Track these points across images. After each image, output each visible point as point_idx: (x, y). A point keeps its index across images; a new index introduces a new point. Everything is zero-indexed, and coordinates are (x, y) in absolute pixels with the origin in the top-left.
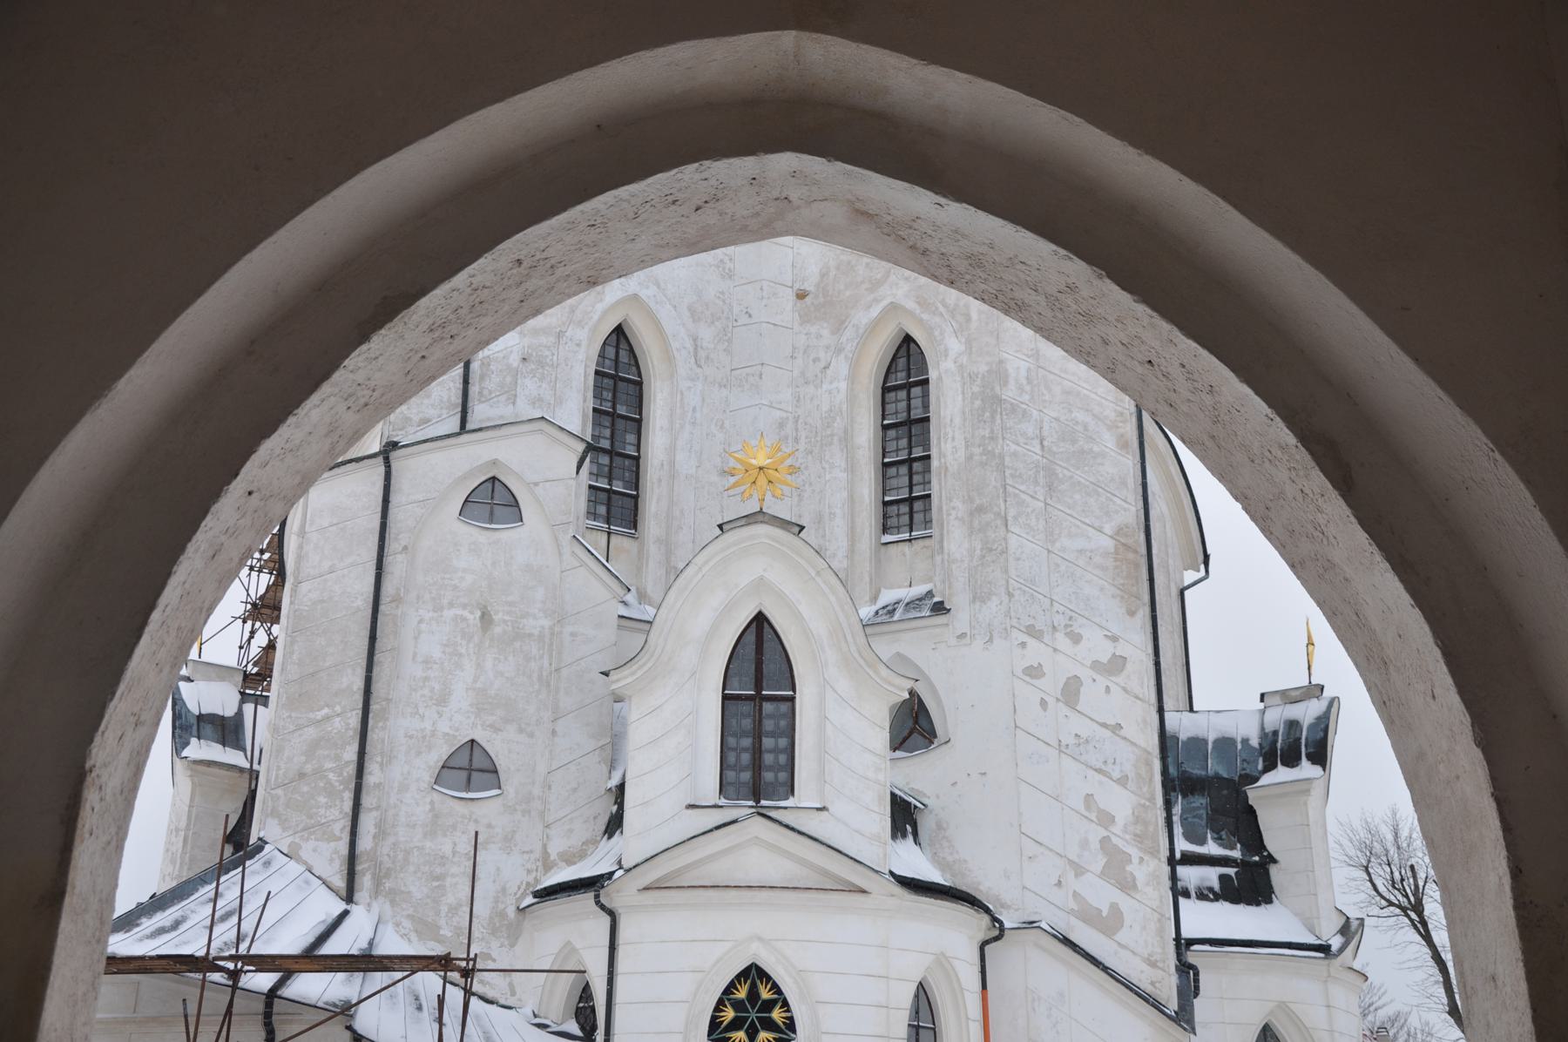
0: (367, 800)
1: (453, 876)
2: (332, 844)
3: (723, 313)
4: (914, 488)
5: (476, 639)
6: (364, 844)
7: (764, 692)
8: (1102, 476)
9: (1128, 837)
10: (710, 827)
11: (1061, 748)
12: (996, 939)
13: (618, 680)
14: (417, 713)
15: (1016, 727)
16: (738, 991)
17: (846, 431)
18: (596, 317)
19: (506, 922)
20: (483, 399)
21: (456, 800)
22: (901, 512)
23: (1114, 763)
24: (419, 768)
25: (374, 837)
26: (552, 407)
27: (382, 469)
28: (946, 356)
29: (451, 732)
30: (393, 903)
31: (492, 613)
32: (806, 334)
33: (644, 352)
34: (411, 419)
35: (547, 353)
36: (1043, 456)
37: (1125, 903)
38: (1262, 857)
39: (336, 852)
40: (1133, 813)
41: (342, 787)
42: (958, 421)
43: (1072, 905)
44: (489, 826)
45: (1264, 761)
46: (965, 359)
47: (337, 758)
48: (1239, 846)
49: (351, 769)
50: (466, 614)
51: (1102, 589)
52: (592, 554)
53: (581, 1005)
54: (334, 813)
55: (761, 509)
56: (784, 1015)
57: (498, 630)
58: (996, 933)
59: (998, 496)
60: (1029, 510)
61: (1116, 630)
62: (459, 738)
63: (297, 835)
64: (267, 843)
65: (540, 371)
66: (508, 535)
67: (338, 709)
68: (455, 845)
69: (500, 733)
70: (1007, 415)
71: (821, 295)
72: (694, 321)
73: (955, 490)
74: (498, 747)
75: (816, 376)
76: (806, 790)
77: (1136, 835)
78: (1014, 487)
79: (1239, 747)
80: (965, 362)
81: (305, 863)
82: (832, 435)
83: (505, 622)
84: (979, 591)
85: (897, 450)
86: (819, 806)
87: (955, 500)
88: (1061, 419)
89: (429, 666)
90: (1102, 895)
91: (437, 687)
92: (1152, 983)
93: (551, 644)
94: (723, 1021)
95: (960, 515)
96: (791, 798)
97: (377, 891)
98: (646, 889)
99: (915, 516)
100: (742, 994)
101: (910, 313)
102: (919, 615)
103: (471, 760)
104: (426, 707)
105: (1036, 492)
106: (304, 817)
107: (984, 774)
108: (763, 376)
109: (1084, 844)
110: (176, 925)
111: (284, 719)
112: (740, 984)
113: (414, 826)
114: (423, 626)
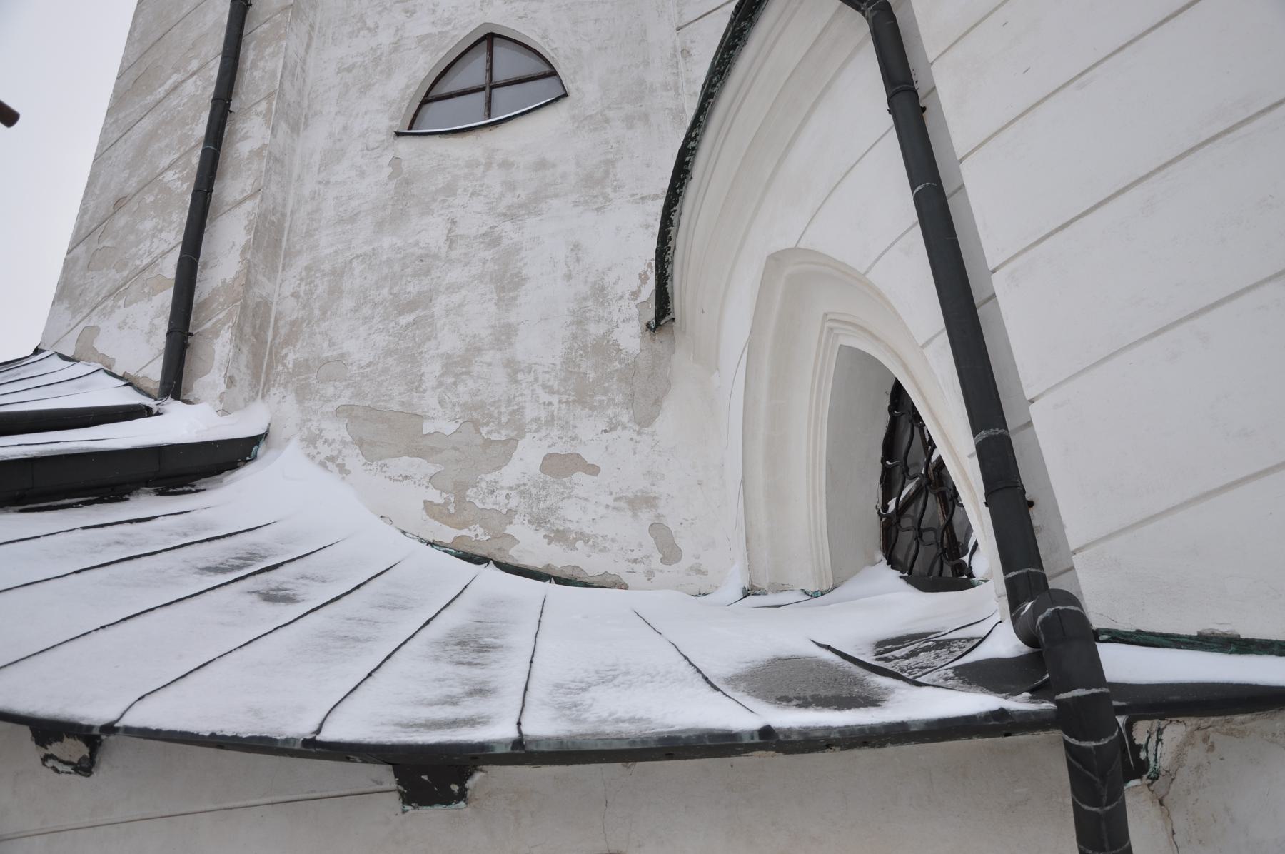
1: (453, 288)
19: (616, 365)
29: (435, 30)
30: (303, 393)
62: (455, 33)
68: (454, 222)
103: (490, 70)
113: (353, 218)
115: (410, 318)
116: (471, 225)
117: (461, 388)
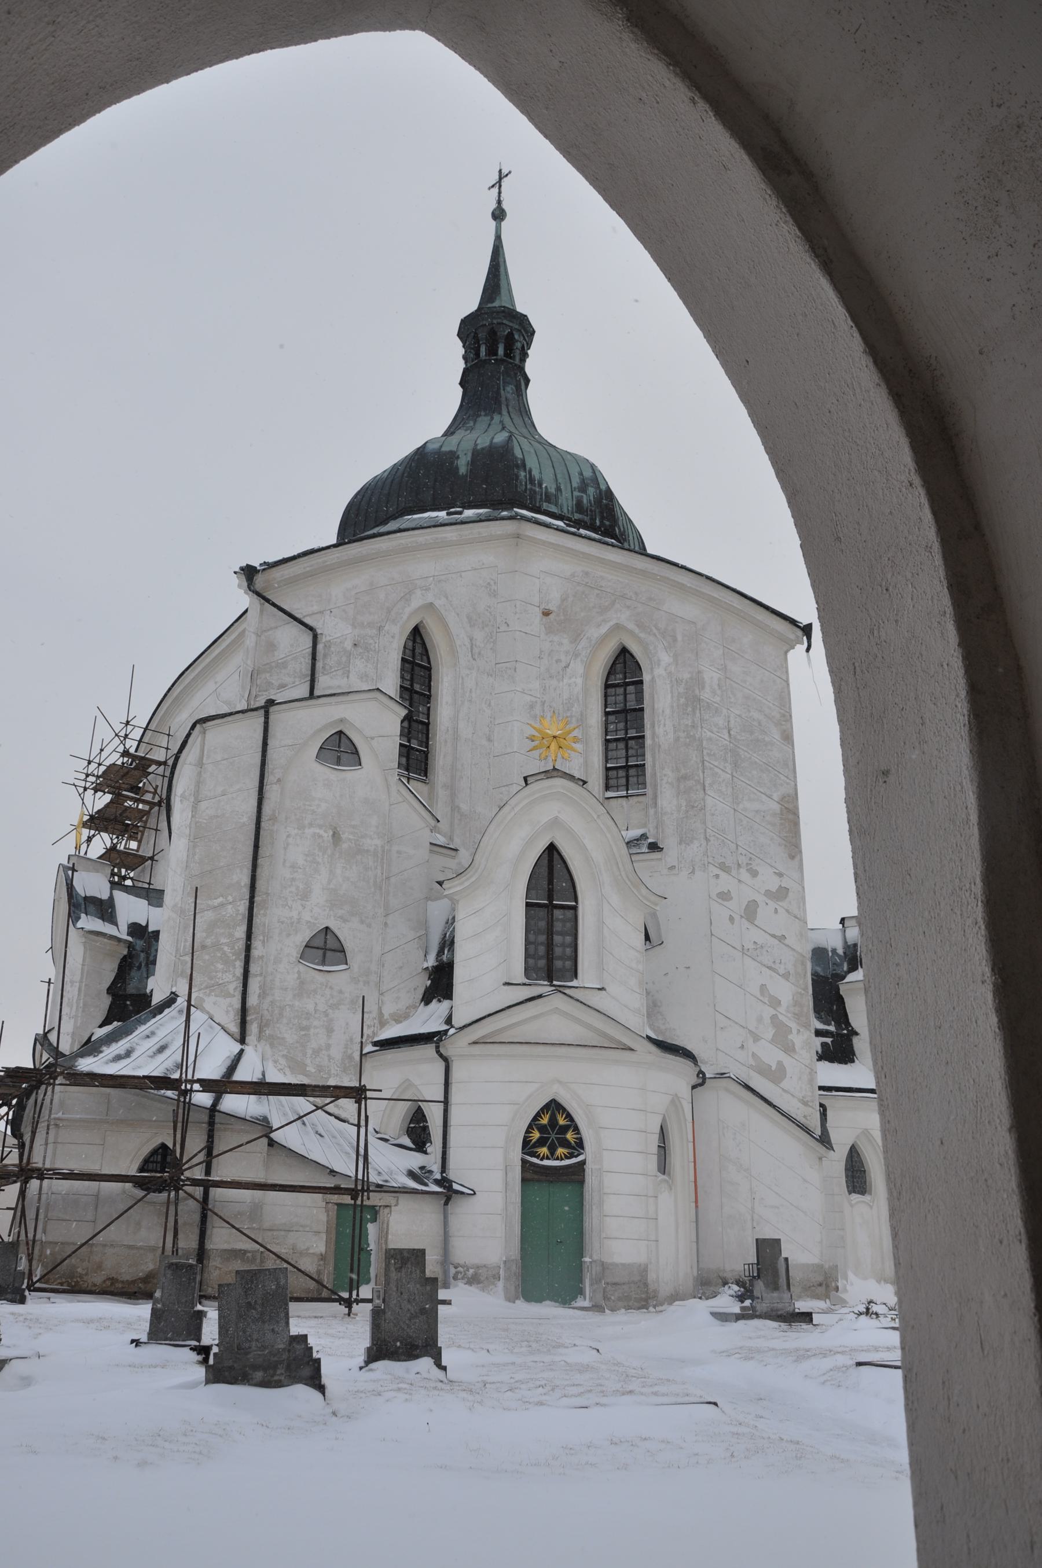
0: (254, 968)
1: (316, 1027)
2: (228, 1000)
3: (490, 621)
4: (630, 759)
5: (329, 852)
6: (252, 1000)
7: (554, 902)
8: (771, 759)
9: (789, 1015)
10: (521, 1000)
11: (744, 951)
12: (702, 1084)
13: (450, 888)
14: (287, 905)
15: (712, 935)
16: (542, 1118)
17: (582, 715)
18: (405, 617)
20: (326, 673)
21: (316, 972)
22: (619, 776)
23: (780, 963)
24: (289, 946)
25: (259, 996)
26: (375, 681)
27: (262, 719)
28: (659, 665)
29: (312, 921)
30: (272, 1045)
31: (341, 833)
32: (550, 642)
33: (434, 646)
34: (272, 684)
35: (371, 641)
36: (730, 742)
37: (787, 1061)
38: (848, 1030)
39: (231, 1005)
40: (793, 998)
41: (234, 957)
42: (668, 712)
43: (752, 1062)
44: (341, 992)
45: (848, 965)
46: (673, 668)
47: (231, 935)
48: (833, 1023)
49: (241, 945)
50: (322, 832)
51: (772, 839)
52: (413, 793)
53: (412, 1125)
54: (228, 977)
55: (554, 767)
56: (575, 1136)
57: (345, 846)
58: (700, 1081)
59: (698, 768)
60: (721, 780)
61: (782, 870)
63: (201, 992)
64: (178, 996)
65: (366, 654)
66: (351, 775)
67: (230, 898)
68: (316, 1004)
69: (347, 923)
70: (704, 710)
71: (561, 614)
72: (470, 626)
73: (666, 762)
74: (345, 933)
75: (559, 673)
76: (587, 976)
77: (795, 1014)
78: (710, 763)
79: (830, 954)
80: (673, 671)
81: (208, 1013)
82: (571, 716)
83: (350, 839)
84: (684, 836)
85: (616, 731)
86: (599, 987)
87: (666, 769)
88: (743, 716)
89: (295, 870)
90: (772, 1055)
91: (301, 886)
92: (805, 1117)
93: (382, 859)
94: (531, 1140)
95: (670, 781)
96: (575, 980)
97: (259, 1039)
98: (475, 1043)
99: (631, 779)
100: (545, 1120)
101: (631, 633)
102: (639, 851)
104: (293, 901)
105: (725, 767)
106: (206, 979)
107: (689, 967)
108: (517, 670)
109: (760, 1019)
110: (128, 1054)
111: (189, 904)
112: (544, 1115)
113: (286, 989)
114: (290, 840)
115: (303, 1033)
116: (322, 1007)
117: (317, 1060)
